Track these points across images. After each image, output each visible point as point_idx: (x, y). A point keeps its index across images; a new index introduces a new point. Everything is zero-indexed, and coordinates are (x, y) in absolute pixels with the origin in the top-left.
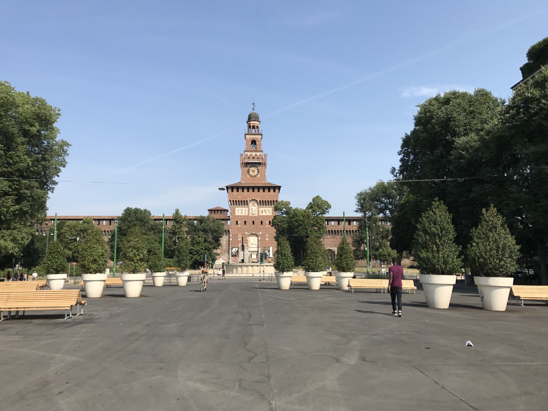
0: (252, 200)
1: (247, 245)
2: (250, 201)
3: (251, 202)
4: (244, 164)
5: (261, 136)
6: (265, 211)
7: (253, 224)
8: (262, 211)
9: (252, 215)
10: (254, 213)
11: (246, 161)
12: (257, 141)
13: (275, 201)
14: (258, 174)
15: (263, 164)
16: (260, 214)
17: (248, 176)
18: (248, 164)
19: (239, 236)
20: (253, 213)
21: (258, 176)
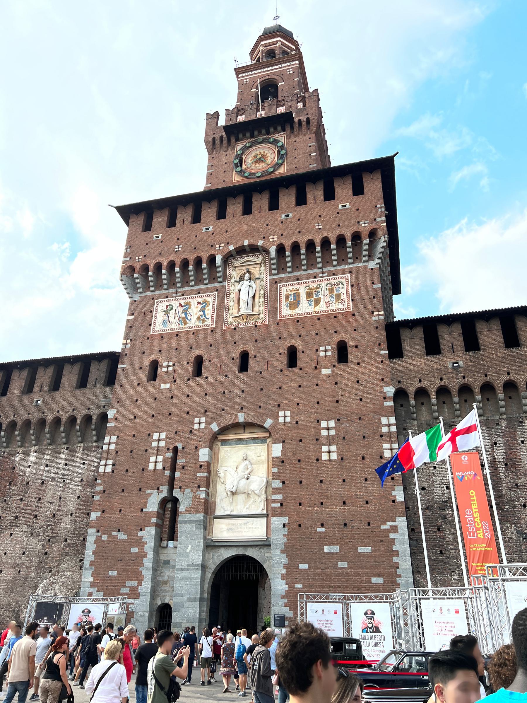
0: (241, 251)
1: (196, 498)
2: (228, 258)
3: (237, 263)
4: (218, 142)
5: (297, 62)
6: (309, 295)
8: (291, 300)
10: (250, 312)
13: (365, 234)
14: (277, 166)
15: (304, 124)
16: (286, 311)
18: (237, 140)
19: (155, 444)
20: (243, 311)
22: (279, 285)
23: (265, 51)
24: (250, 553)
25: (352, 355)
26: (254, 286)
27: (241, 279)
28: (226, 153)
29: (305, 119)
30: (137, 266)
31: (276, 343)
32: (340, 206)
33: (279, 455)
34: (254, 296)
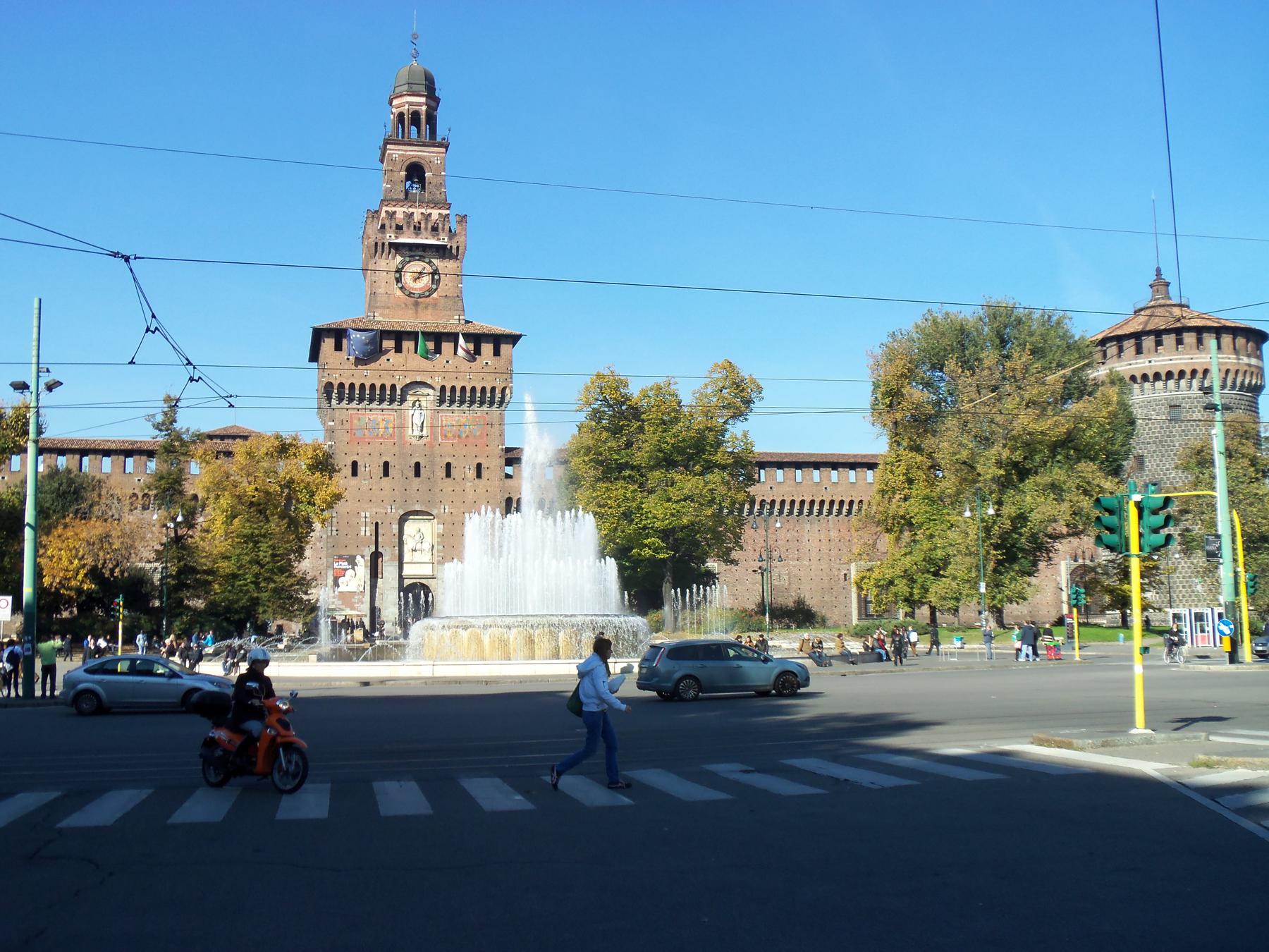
4: (380, 249)
5: (444, 150)
7: (417, 474)
9: (414, 441)
11: (391, 237)
12: (426, 170)
14: (431, 291)
15: (454, 251)
17: (399, 293)
20: (417, 433)
21: (435, 295)
22: (440, 414)
23: (410, 112)
24: (423, 581)
25: (484, 473)
26: (423, 414)
27: (414, 405)
28: (388, 261)
29: (455, 247)
30: (336, 384)
31: (438, 459)
32: (485, 362)
33: (441, 532)
34: (423, 422)
